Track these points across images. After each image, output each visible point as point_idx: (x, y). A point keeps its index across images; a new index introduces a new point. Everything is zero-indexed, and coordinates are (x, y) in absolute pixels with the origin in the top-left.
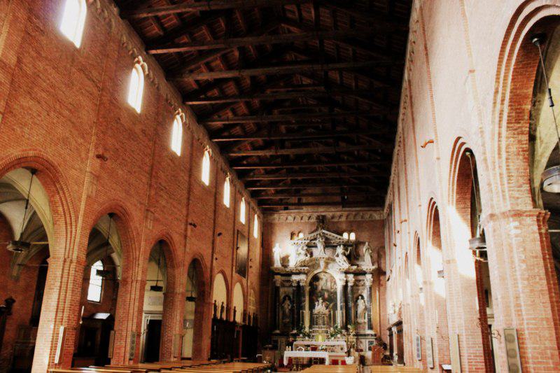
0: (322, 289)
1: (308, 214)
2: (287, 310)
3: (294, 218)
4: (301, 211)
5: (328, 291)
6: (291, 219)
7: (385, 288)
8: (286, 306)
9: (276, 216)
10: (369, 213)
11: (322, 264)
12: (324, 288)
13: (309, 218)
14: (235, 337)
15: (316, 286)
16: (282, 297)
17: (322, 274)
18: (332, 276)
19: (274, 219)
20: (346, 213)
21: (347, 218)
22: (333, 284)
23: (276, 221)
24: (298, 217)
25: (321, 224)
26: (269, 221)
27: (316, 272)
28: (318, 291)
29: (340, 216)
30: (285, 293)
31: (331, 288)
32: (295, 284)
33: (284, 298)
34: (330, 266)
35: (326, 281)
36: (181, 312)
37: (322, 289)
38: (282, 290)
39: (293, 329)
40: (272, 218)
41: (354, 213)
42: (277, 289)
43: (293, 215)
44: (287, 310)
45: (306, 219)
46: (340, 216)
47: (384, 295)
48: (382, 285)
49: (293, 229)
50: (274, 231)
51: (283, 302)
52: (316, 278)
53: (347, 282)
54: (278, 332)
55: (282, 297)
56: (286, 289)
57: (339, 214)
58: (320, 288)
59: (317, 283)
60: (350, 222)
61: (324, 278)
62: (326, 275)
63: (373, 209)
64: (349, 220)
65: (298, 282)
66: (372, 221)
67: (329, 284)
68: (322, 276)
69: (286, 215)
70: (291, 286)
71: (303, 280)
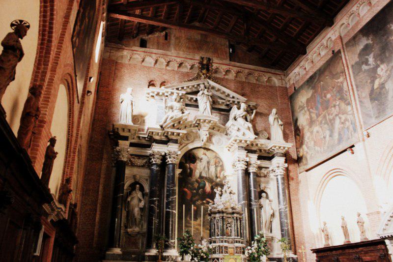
0: (201, 177)
1: (179, 60)
2: (136, 210)
3: (156, 61)
4: (169, 53)
5: (210, 180)
6: (150, 61)
7: (298, 183)
8: (135, 202)
9: (126, 53)
10: (268, 75)
11: (204, 133)
12: (204, 175)
13: (181, 65)
14: (37, 254)
15: (191, 170)
16: (127, 184)
17: (202, 151)
18: (217, 157)
19: (122, 57)
20: (236, 69)
21: (236, 77)
22: (219, 169)
23: (126, 61)
24: (163, 61)
25: (204, 71)
26: (114, 58)
27: (191, 146)
28: (194, 179)
29: (227, 72)
30: (134, 177)
31: (217, 177)
32: (156, 160)
33: (133, 187)
34: (214, 139)
35: (208, 163)
36: (77, 221)
37: (201, 177)
38: (128, 171)
39: (149, 247)
40: (120, 54)
41: (246, 71)
42: (121, 166)
43: (154, 56)
44: (136, 210)
45: (174, 66)
46: (227, 72)
47: (296, 195)
48: (293, 179)
49: (152, 77)
50: (119, 74)
51: (130, 194)
52: (190, 157)
53: (248, 164)
54: (118, 251)
55: (127, 184)
56: (136, 171)
57: (225, 67)
58: (197, 174)
59: (192, 166)
60: (240, 82)
61: (205, 159)
62: (208, 153)
63: (273, 71)
64: (238, 79)
65: (164, 158)
66: (271, 87)
67: (212, 169)
68: (200, 153)
69: (143, 54)
70: (149, 165)
71: (175, 153)
